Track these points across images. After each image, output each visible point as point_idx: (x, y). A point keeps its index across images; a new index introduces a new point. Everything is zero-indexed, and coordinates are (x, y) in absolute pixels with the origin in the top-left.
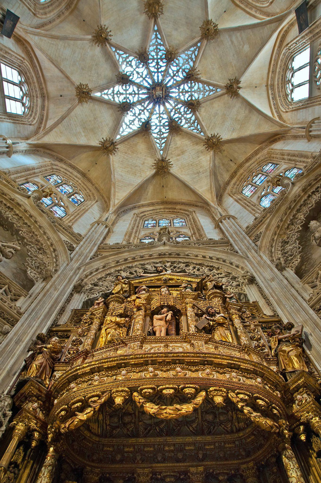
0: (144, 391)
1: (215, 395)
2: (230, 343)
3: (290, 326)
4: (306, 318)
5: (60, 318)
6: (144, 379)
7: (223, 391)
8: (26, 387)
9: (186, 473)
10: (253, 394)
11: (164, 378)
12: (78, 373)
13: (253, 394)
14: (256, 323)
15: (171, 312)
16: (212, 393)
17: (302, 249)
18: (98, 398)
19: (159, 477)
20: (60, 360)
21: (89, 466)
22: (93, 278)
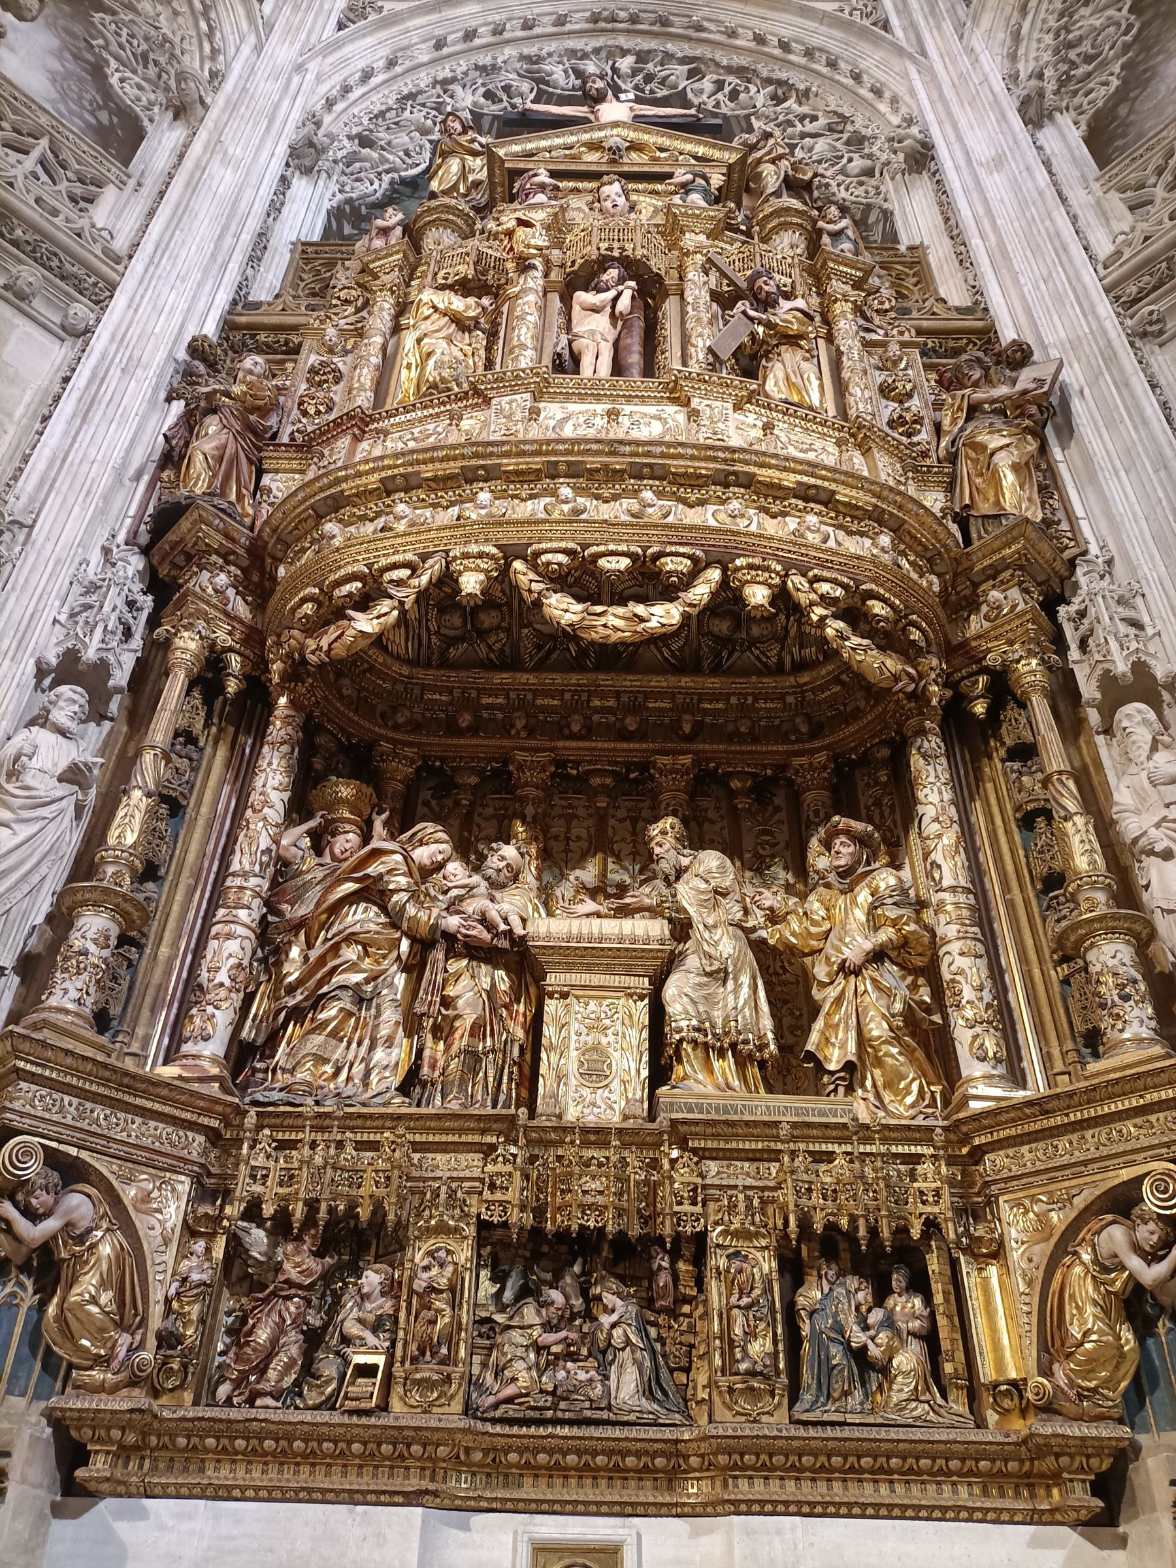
0: (544, 558)
1: (748, 582)
2: (811, 408)
3: (1020, 356)
4: (1081, 334)
5: (254, 277)
6: (544, 521)
7: (775, 571)
8: (184, 524)
9: (645, 767)
10: (858, 584)
11: (605, 521)
12: (342, 492)
13: (858, 584)
14: (906, 337)
15: (633, 284)
16: (739, 575)
17: (1140, 31)
18: (409, 572)
19: (574, 772)
20: (275, 436)
21: (389, 740)
22: (356, 111)
